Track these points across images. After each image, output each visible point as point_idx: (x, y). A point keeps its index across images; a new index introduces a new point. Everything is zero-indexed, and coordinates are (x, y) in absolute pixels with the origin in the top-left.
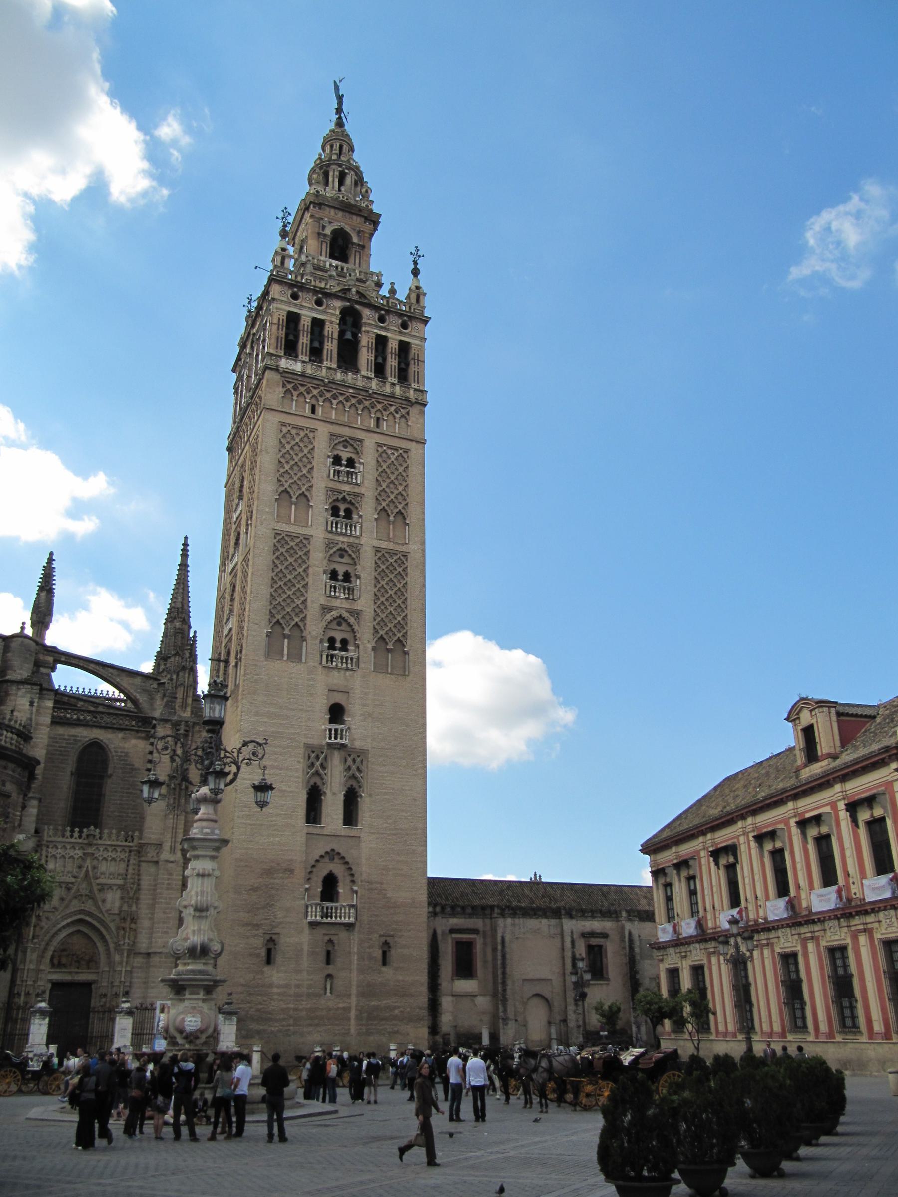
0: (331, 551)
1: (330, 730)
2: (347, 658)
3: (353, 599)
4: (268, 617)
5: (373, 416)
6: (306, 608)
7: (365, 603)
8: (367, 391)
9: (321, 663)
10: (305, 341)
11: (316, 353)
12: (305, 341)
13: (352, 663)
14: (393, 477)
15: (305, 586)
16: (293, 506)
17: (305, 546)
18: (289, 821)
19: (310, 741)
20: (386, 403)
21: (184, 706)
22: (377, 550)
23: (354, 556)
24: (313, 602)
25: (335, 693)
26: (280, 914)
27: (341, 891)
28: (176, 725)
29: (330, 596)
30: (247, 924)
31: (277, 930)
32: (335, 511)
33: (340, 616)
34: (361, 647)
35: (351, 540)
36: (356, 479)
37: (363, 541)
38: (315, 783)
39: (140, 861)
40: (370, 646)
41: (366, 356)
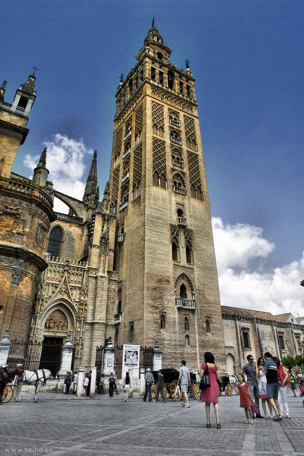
0: (173, 149)
1: (179, 219)
6: (166, 168)
7: (186, 170)
11: (161, 81)
14: (190, 127)
15: (165, 159)
17: (164, 145)
18: (166, 258)
19: (172, 223)
21: (107, 209)
22: (188, 152)
24: (168, 166)
25: (179, 205)
26: (166, 303)
28: (103, 216)
30: (152, 307)
31: (165, 311)
33: (178, 174)
34: (187, 187)
35: (179, 146)
38: (174, 242)
39: (88, 276)
40: (189, 187)
41: (177, 87)
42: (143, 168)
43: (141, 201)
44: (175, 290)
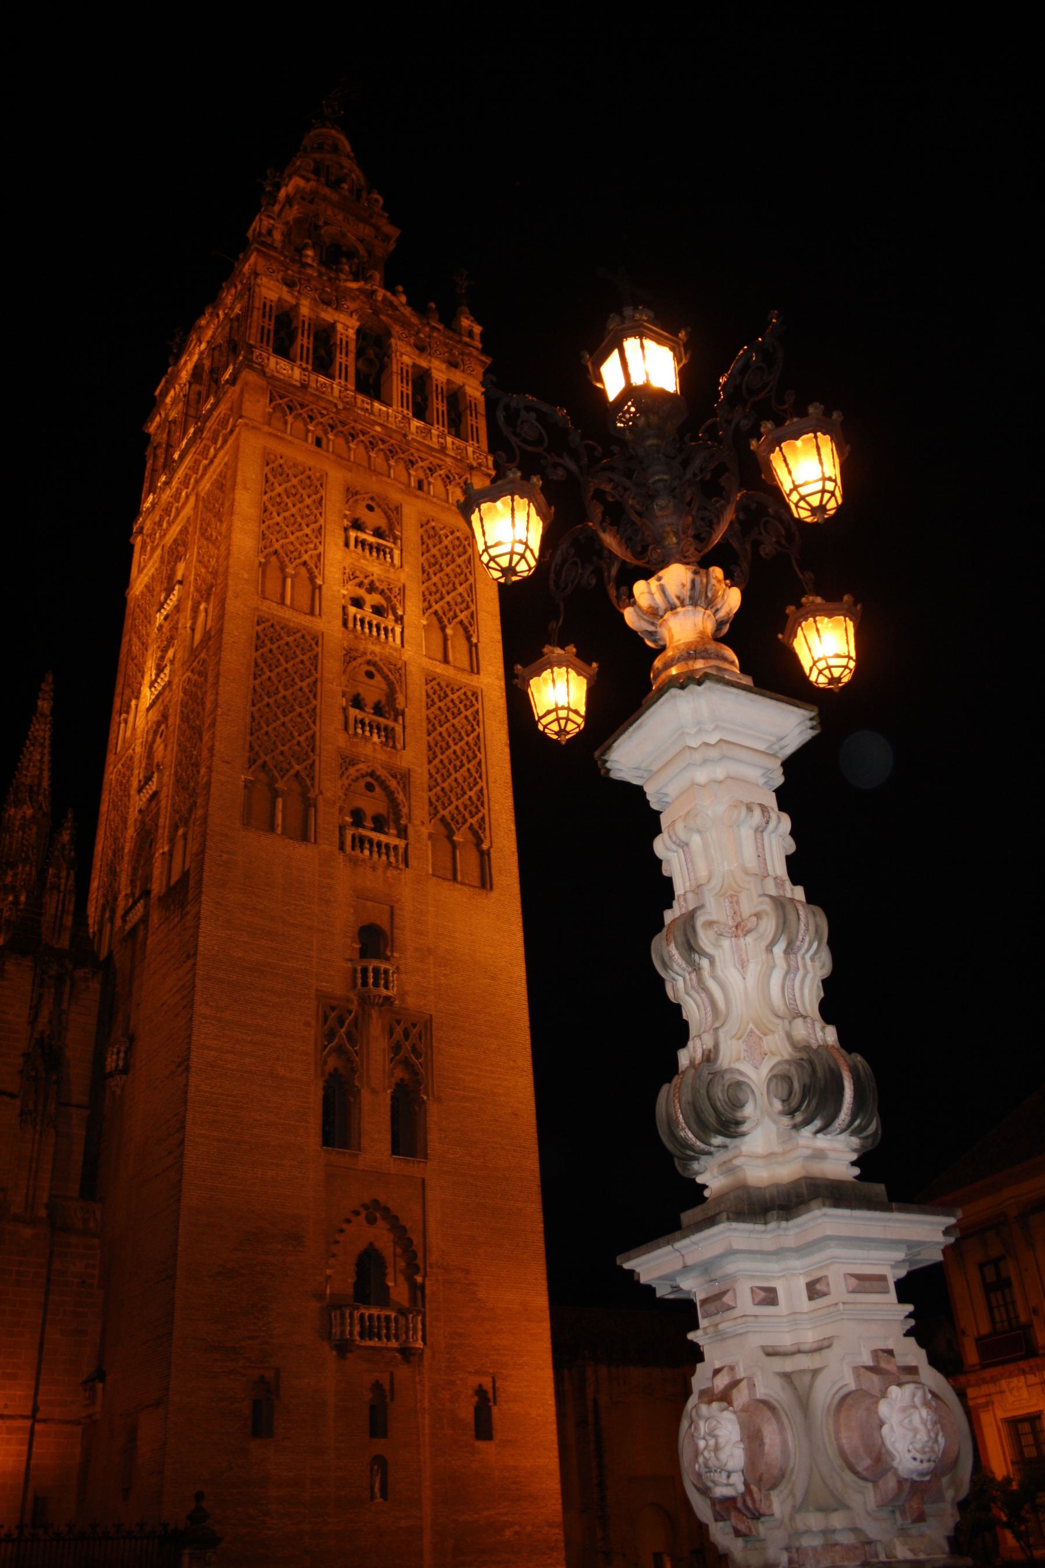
2: (387, 846)
3: (394, 747)
4: (247, 754)
5: (412, 472)
7: (413, 757)
8: (405, 436)
9: (342, 848)
10: (305, 342)
12: (305, 342)
13: (396, 856)
16: (289, 581)
20: (431, 459)
23: (391, 677)
25: (369, 903)
27: (391, 1284)
29: (356, 734)
32: (358, 603)
33: (372, 774)
36: (392, 558)
37: (408, 653)
38: (336, 1070)
40: (425, 831)
41: (399, 387)
42: (205, 753)
43: (190, 896)
44: (329, 1272)
